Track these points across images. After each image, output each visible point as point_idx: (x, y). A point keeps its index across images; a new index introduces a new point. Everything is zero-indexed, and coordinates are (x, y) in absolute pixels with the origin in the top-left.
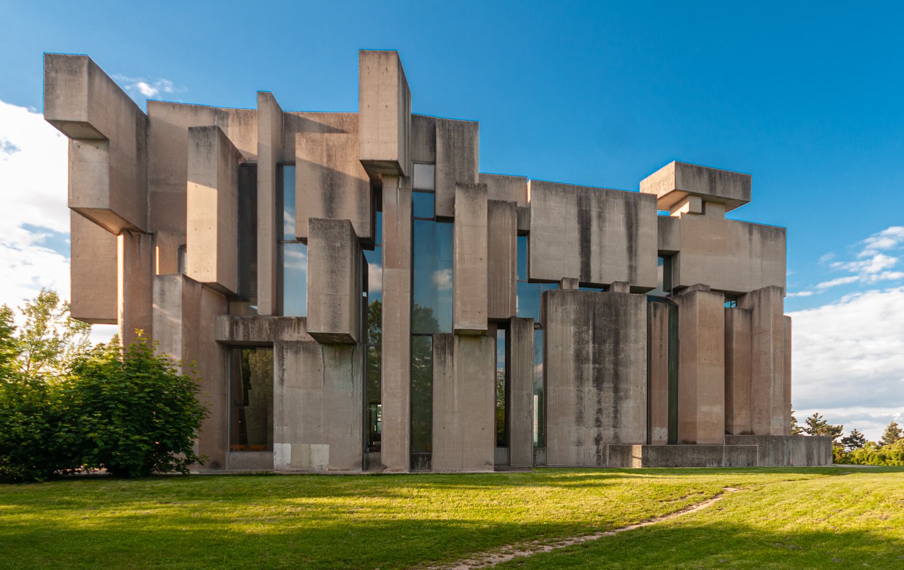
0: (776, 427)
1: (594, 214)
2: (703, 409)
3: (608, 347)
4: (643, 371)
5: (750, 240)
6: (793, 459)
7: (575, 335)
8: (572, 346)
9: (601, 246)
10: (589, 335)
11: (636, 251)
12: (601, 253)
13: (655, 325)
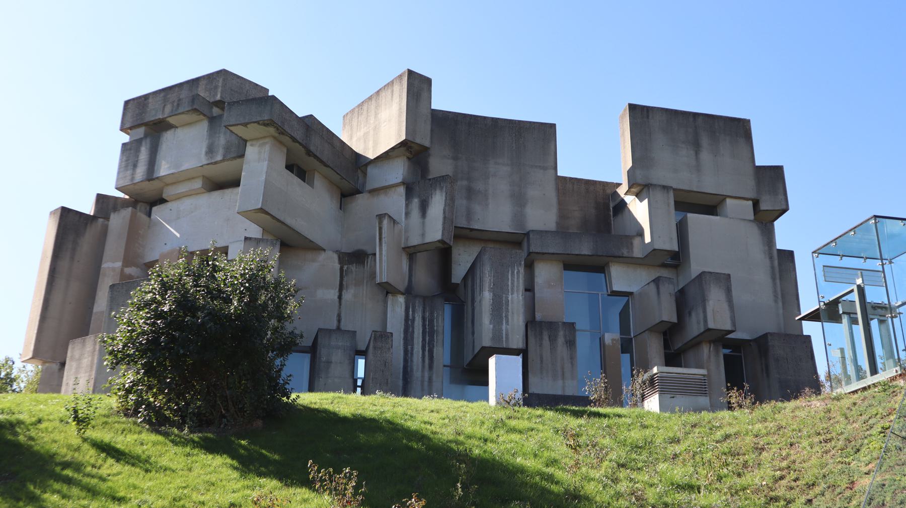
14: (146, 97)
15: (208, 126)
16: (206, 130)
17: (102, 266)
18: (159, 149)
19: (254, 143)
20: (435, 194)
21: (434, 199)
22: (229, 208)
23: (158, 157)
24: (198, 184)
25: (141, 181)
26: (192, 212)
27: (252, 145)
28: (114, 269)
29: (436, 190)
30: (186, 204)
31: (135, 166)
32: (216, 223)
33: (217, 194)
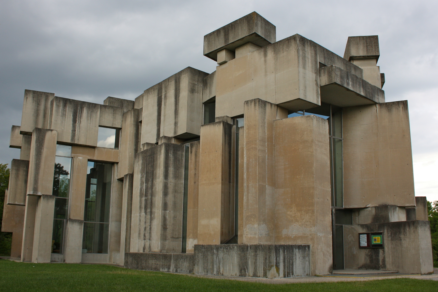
0: (249, 236)
1: (163, 97)
2: (203, 222)
3: (150, 183)
4: (160, 197)
5: (265, 61)
6: (223, 267)
7: (140, 179)
8: (139, 187)
9: (165, 116)
10: (144, 179)
11: (178, 111)
12: (164, 120)
13: (191, 159)
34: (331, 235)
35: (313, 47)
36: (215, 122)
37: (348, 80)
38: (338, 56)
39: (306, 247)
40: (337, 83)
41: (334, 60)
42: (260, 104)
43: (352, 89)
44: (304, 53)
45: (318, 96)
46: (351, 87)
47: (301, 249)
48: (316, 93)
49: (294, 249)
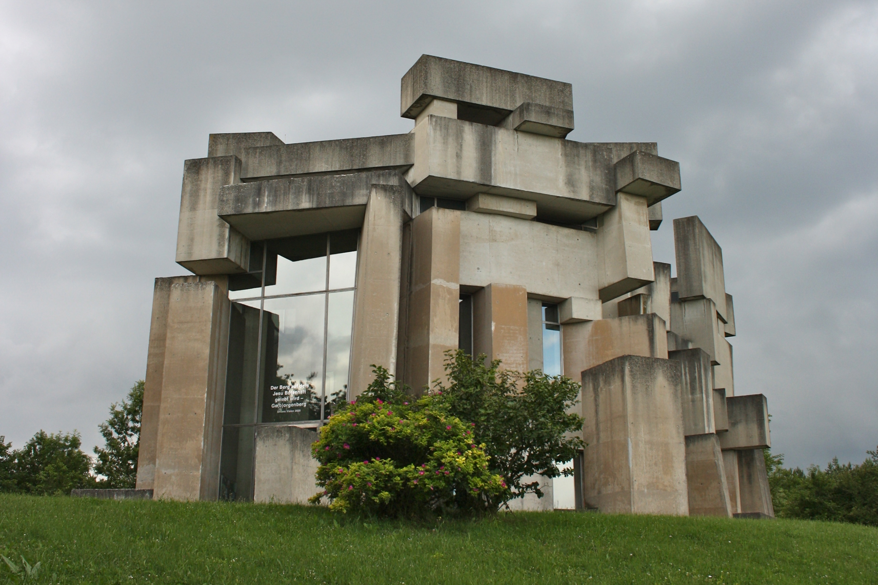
14: (463, 65)
15: (562, 148)
16: (560, 153)
17: (433, 282)
18: (493, 148)
19: (629, 197)
20: (660, 281)
21: (658, 285)
22: (557, 251)
23: (493, 159)
24: (532, 211)
25: (473, 182)
26: (512, 239)
27: (627, 200)
28: (449, 291)
29: (660, 276)
30: (503, 225)
31: (459, 156)
32: (544, 264)
33: (539, 227)
34: (199, 470)
35: (222, 164)
36: (259, 310)
37: (259, 198)
38: (324, 143)
39: (146, 492)
40: (229, 213)
41: (310, 155)
42: (158, 285)
43: (269, 209)
44: (197, 185)
45: (222, 243)
46: (266, 207)
47: (131, 496)
48: (219, 239)
49: (115, 495)
